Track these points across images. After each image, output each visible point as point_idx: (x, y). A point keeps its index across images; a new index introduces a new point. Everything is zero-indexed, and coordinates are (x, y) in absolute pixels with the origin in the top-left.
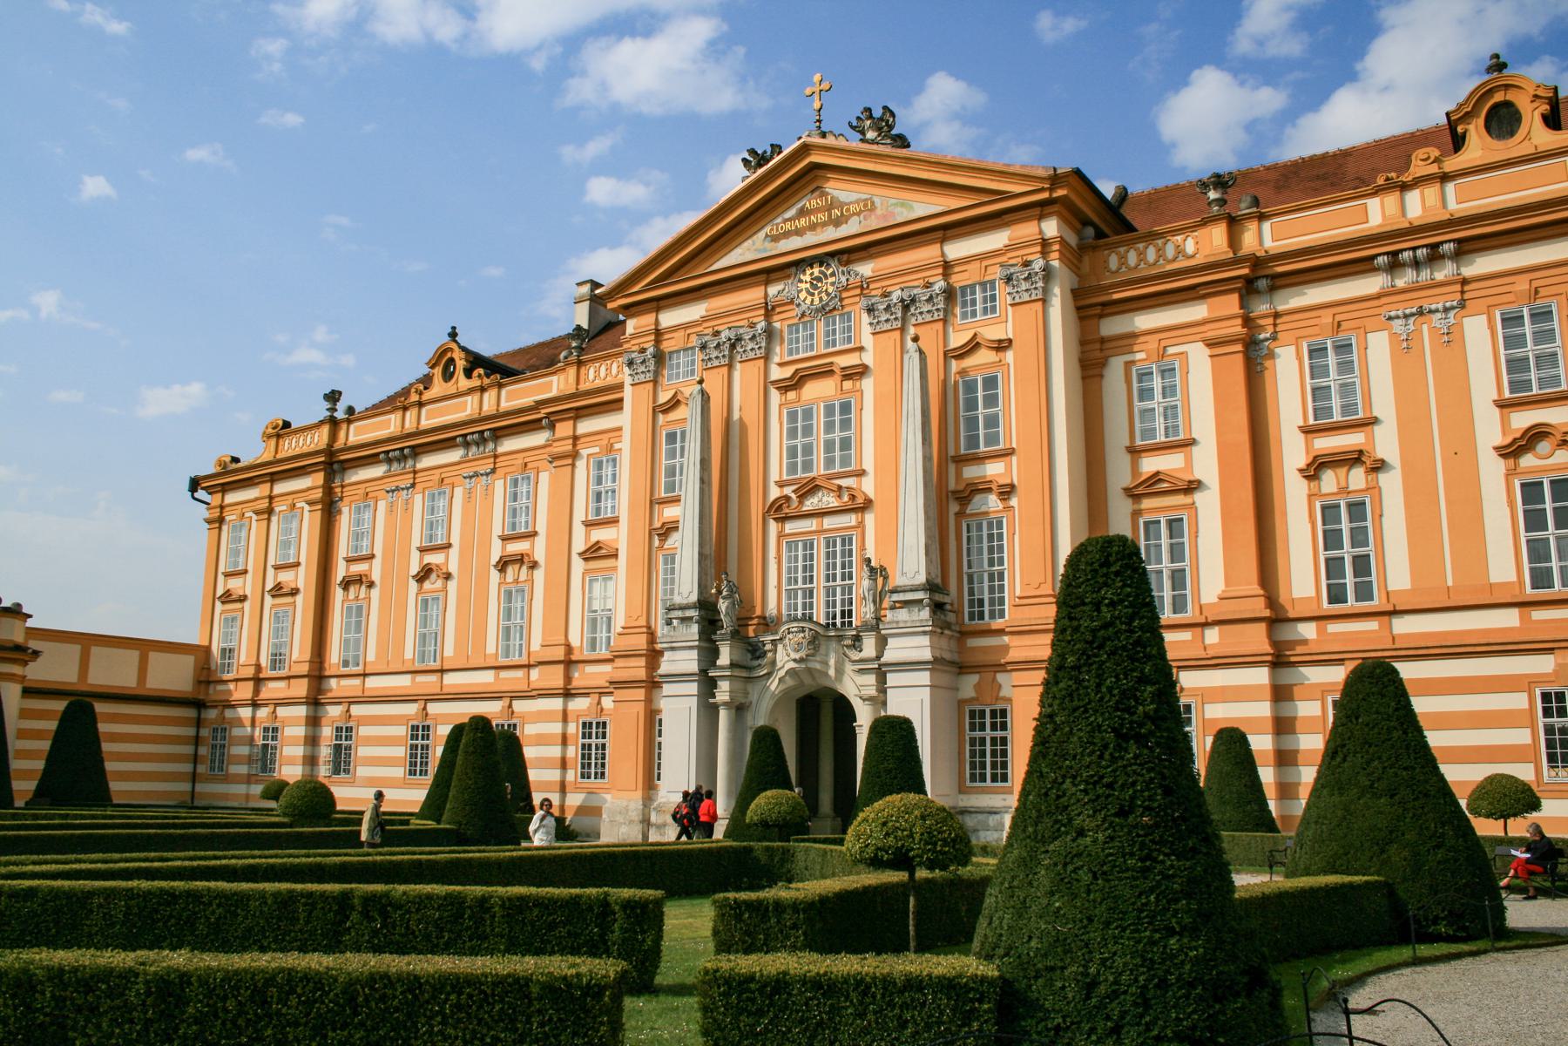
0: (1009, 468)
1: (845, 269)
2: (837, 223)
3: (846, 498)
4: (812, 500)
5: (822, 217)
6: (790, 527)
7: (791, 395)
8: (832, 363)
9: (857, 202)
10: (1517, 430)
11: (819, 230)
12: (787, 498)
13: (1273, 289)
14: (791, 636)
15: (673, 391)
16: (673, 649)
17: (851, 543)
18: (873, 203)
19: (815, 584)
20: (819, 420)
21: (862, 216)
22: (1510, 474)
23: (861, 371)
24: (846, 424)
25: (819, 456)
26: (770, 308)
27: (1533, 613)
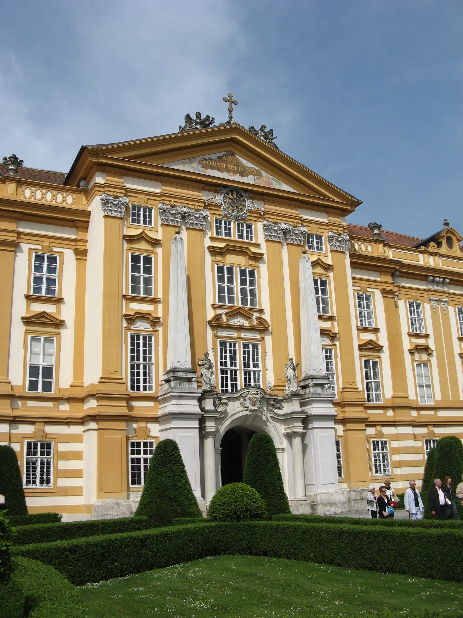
0: (333, 325)
1: (251, 201)
2: (242, 175)
3: (255, 322)
7: (219, 258)
8: (248, 248)
11: (231, 174)
12: (221, 315)
13: (399, 276)
14: (249, 396)
15: (140, 231)
16: (180, 397)
18: (261, 173)
19: (238, 367)
20: (237, 276)
21: (255, 177)
23: (257, 258)
24: (252, 283)
26: (207, 204)
27: (421, 411)
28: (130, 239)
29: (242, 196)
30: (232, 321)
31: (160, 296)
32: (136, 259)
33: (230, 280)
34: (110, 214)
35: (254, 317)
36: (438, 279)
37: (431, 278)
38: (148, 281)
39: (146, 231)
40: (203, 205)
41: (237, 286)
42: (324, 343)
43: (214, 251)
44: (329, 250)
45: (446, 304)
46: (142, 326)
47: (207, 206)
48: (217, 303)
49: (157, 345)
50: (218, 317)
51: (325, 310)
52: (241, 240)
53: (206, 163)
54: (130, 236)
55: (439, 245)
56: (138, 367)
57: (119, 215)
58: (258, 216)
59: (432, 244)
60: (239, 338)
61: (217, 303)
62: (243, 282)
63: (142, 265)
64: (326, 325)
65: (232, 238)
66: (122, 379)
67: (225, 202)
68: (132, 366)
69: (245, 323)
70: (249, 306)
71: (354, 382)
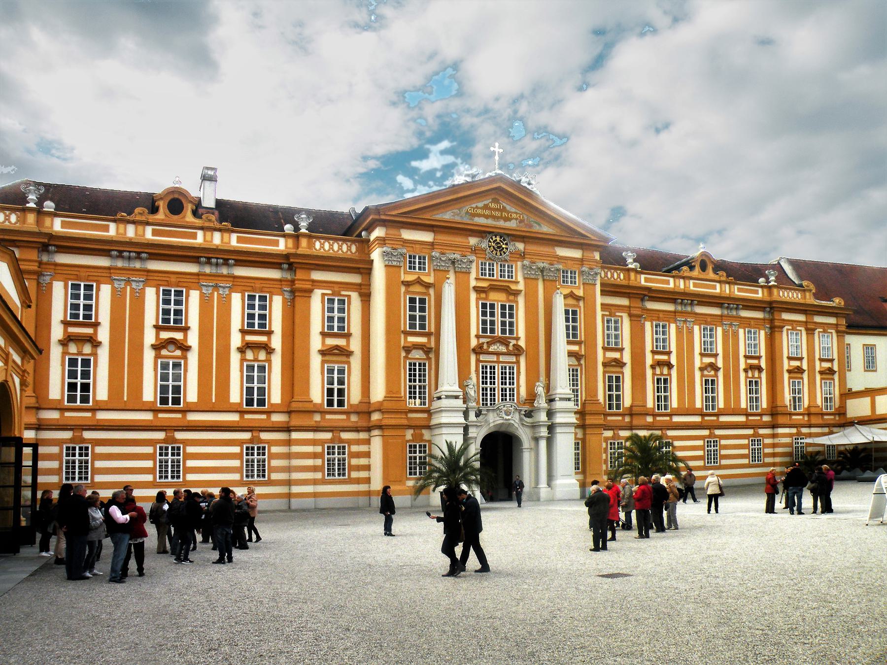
0: (580, 348)
2: (507, 219)
3: (511, 348)
4: (494, 347)
5: (498, 214)
6: (482, 358)
7: (483, 295)
8: (508, 286)
9: (516, 213)
10: (705, 363)
12: (483, 343)
17: (513, 369)
19: (496, 385)
20: (498, 311)
22: (702, 376)
23: (516, 293)
25: (498, 328)
28: (407, 284)
29: (504, 240)
30: (493, 348)
31: (433, 330)
32: (412, 300)
33: (492, 314)
34: (390, 263)
35: (511, 344)
36: (686, 301)
37: (680, 301)
38: (423, 318)
39: (420, 276)
40: (470, 250)
41: (498, 319)
42: (571, 363)
43: (477, 289)
44: (581, 284)
45: (692, 323)
46: (417, 354)
47: (475, 250)
48: (481, 334)
49: (430, 369)
50: (480, 346)
51: (575, 336)
52: (502, 279)
53: (474, 211)
54: (407, 281)
55: (692, 268)
56: (415, 387)
57: (398, 264)
58: (518, 256)
59: (685, 268)
60: (498, 362)
61: (481, 334)
62: (503, 315)
63: (418, 305)
64: (575, 348)
65: (495, 278)
66: (402, 397)
67: (490, 247)
68: (410, 387)
69: (503, 349)
70: (508, 335)
71: (596, 395)
